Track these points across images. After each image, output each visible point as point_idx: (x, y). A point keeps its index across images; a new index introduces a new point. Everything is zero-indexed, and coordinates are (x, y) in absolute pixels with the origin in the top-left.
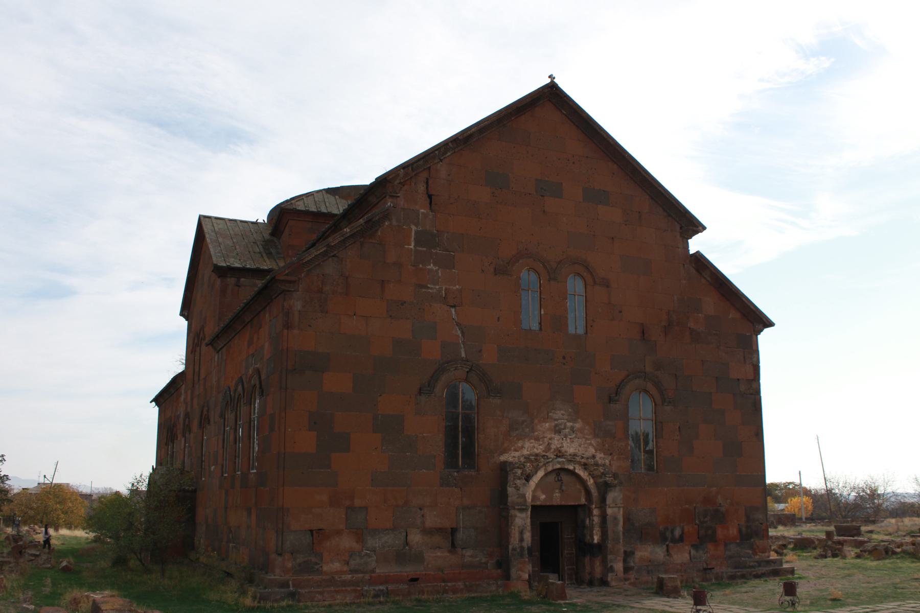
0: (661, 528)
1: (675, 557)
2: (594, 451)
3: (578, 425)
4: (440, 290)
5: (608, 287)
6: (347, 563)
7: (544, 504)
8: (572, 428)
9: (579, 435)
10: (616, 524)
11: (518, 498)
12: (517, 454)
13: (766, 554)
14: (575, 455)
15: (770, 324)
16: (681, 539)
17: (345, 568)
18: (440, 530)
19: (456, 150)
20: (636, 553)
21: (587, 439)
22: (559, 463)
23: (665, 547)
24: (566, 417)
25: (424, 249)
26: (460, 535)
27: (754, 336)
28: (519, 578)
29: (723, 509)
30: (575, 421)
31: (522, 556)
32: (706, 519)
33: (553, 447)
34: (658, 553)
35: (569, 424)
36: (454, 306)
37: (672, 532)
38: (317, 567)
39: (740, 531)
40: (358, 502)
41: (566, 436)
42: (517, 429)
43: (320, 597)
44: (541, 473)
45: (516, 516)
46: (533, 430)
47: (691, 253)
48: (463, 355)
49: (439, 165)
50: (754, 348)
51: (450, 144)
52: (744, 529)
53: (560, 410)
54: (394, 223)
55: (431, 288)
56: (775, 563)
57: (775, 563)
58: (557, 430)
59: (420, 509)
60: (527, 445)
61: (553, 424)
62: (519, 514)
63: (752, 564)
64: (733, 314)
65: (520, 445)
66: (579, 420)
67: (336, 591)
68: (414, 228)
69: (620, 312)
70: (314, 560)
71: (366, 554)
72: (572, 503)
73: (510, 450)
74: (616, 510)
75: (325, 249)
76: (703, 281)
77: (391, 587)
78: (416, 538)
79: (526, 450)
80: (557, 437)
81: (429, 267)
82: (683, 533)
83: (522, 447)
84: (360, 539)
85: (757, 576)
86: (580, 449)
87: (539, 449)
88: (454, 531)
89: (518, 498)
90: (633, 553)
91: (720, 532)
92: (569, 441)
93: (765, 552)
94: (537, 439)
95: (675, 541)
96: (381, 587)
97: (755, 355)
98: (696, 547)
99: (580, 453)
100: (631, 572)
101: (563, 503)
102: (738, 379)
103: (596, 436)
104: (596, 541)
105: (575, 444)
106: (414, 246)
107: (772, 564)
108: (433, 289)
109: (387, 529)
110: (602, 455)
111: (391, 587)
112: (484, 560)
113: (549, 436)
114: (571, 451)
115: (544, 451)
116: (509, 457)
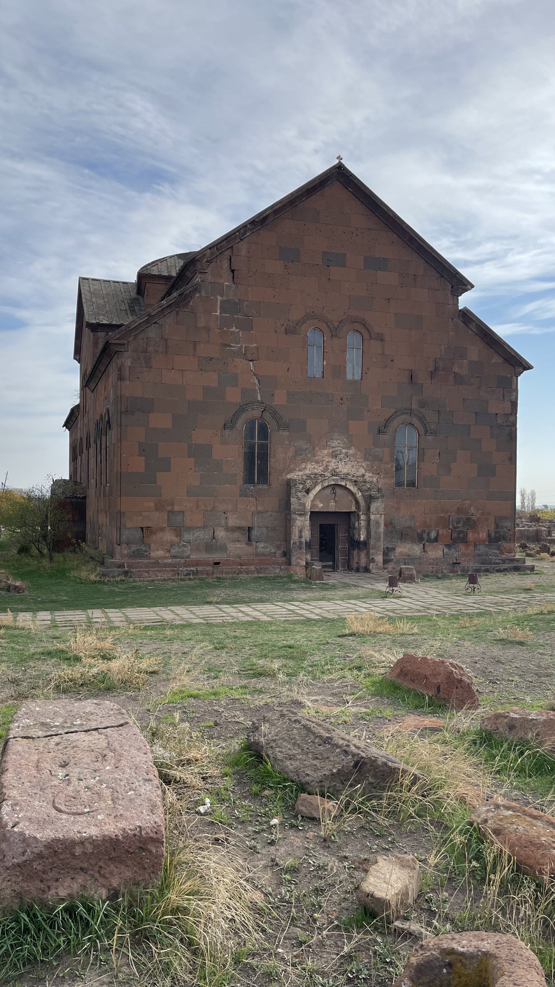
1: (430, 553)
2: (364, 471)
3: (351, 452)
4: (240, 348)
5: (382, 340)
7: (321, 511)
9: (352, 459)
11: (299, 506)
12: (300, 473)
13: (512, 554)
14: (348, 474)
15: (527, 367)
16: (436, 540)
18: (239, 528)
19: (255, 230)
20: (396, 549)
21: (358, 462)
22: (334, 480)
23: (421, 545)
24: (342, 445)
25: (228, 315)
26: (255, 533)
27: (515, 378)
29: (474, 518)
30: (349, 448)
31: (300, 548)
32: (458, 525)
33: (330, 468)
34: (416, 549)
35: (344, 451)
36: (252, 361)
37: (428, 534)
38: (146, 553)
39: (489, 535)
40: (176, 508)
41: (341, 460)
42: (301, 455)
43: (146, 575)
44: (318, 488)
45: (296, 519)
46: (314, 455)
47: (460, 309)
48: (259, 398)
49: (240, 244)
50: (514, 387)
51: (248, 226)
52: (493, 535)
54: (204, 294)
55: (234, 347)
58: (334, 455)
59: (225, 513)
60: (309, 466)
61: (331, 451)
62: (298, 518)
63: (496, 562)
64: (496, 359)
67: (158, 571)
68: (219, 298)
69: (392, 361)
70: (144, 548)
71: (183, 545)
72: (345, 511)
73: (295, 470)
74: (378, 516)
75: (147, 318)
76: (470, 332)
77: (200, 568)
79: (308, 471)
80: (334, 460)
81: (232, 330)
82: (438, 534)
83: (305, 468)
84: (179, 534)
85: (499, 571)
86: (353, 470)
87: (319, 470)
88: (250, 529)
89: (299, 506)
90: (394, 549)
91: (471, 536)
92: (343, 464)
93: (512, 552)
94: (317, 462)
95: (430, 541)
96: (192, 569)
97: (514, 394)
98: (448, 546)
99: (352, 473)
100: (390, 563)
101: (337, 510)
103: (366, 459)
104: (362, 539)
106: (220, 313)
108: (235, 347)
109: (199, 528)
110: (371, 475)
111: (200, 568)
112: (273, 551)
113: (327, 460)
114: (345, 471)
115: (322, 471)
116: (294, 476)
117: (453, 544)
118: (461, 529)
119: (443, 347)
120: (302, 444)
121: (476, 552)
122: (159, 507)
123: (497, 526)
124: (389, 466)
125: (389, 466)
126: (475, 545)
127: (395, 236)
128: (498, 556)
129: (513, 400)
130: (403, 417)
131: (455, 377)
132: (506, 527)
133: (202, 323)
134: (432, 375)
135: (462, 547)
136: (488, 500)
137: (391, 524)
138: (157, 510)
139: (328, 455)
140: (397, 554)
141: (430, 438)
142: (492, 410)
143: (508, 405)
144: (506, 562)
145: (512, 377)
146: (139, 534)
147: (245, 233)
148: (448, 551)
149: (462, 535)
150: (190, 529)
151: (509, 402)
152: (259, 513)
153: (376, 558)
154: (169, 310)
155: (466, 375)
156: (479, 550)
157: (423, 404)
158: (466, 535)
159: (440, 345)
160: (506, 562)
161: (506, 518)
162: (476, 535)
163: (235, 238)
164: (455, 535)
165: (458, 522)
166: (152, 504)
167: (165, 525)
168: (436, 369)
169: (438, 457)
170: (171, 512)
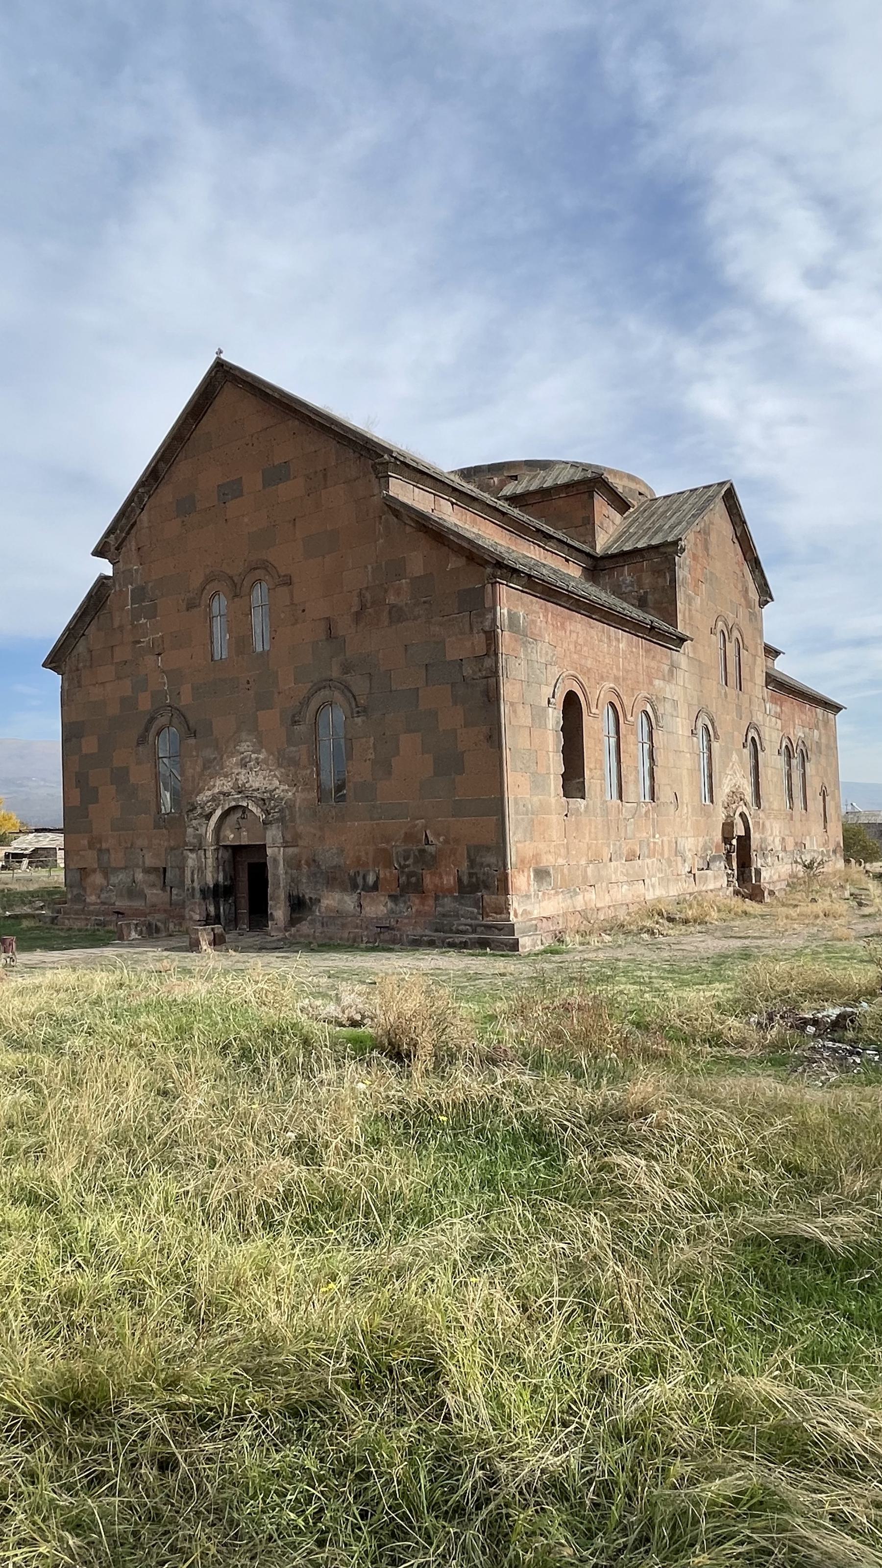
0: (352, 872)
1: (367, 909)
3: (261, 756)
6: (99, 897)
8: (257, 759)
9: (264, 766)
10: (276, 867)
12: (210, 793)
13: (504, 916)
16: (375, 887)
17: (98, 901)
18: (156, 869)
23: (355, 896)
24: (251, 748)
28: (191, 918)
29: (431, 849)
30: (258, 752)
31: (193, 896)
32: (407, 863)
34: (349, 902)
37: (364, 878)
39: (460, 880)
40: (104, 846)
42: (209, 768)
52: (465, 879)
53: (246, 741)
54: (118, 588)
56: (500, 930)
57: (500, 930)
62: (190, 855)
63: (461, 928)
64: (455, 562)
65: (212, 784)
66: (263, 750)
68: (130, 586)
69: (304, 611)
71: (111, 890)
78: (140, 876)
80: (244, 771)
82: (378, 878)
83: (214, 786)
84: (106, 876)
85: (452, 945)
88: (165, 869)
90: (319, 901)
93: (501, 913)
94: (226, 776)
95: (368, 889)
97: (489, 616)
98: (394, 898)
101: (250, 843)
102: (461, 660)
103: (280, 766)
105: (260, 778)
107: (496, 931)
110: (287, 787)
113: (236, 771)
114: (256, 785)
117: (402, 896)
118: (412, 869)
119: (369, 567)
120: (209, 753)
121: (438, 909)
122: (91, 846)
123: (472, 863)
124: (308, 772)
125: (308, 772)
126: (437, 898)
127: (297, 423)
128: (476, 919)
129: (487, 629)
130: (322, 692)
131: (390, 613)
132: (489, 865)
133: (116, 624)
134: (358, 616)
135: (415, 900)
136: (453, 816)
137: (314, 861)
138: (90, 848)
139: (236, 764)
140: (323, 909)
141: (359, 720)
142: (452, 654)
143: (479, 640)
144: (479, 929)
145: (484, 586)
146: (77, 876)
147: (141, 500)
148: (393, 906)
149: (413, 880)
150: (116, 870)
151: (482, 635)
152: (172, 849)
153: (275, 914)
154: (88, 620)
155: (406, 604)
156: (443, 906)
157: (346, 669)
158: (421, 880)
159: (366, 567)
160: (479, 929)
161: (488, 849)
162: (437, 880)
163: (133, 510)
164: (403, 879)
165: (406, 858)
166: (86, 842)
167: (96, 866)
168: (363, 607)
169: (371, 751)
170: (100, 850)
